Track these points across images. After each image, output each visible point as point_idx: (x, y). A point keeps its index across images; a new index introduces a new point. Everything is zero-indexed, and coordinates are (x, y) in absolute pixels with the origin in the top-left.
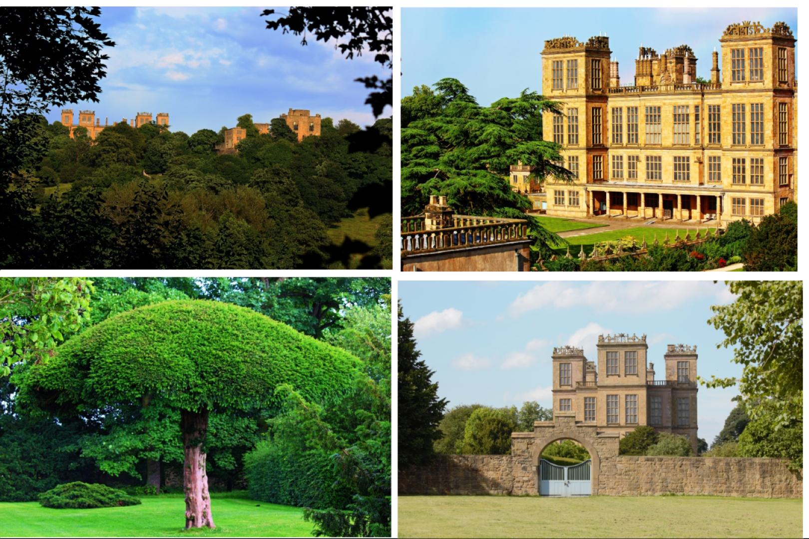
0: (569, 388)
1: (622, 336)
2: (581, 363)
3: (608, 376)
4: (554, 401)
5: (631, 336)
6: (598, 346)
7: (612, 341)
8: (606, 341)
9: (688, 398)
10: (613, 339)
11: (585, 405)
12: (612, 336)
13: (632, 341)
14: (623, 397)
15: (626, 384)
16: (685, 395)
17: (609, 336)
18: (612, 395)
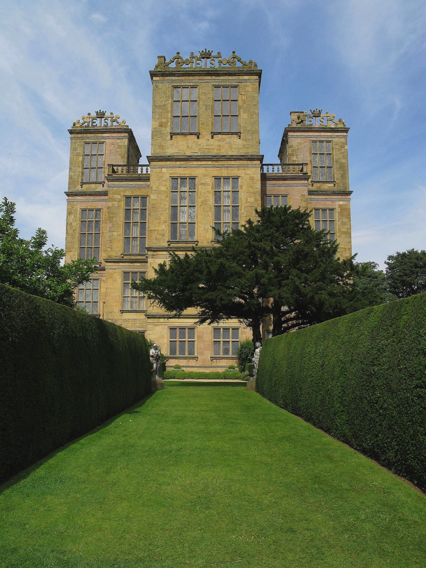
0: (100, 188)
1: (206, 55)
2: (126, 141)
3: (172, 135)
4: (69, 213)
5: (227, 56)
6: (153, 75)
7: (184, 66)
8: (173, 65)
9: (332, 210)
10: (187, 62)
11: (127, 211)
12: (186, 57)
13: (227, 65)
14: (210, 181)
15: (214, 152)
16: (329, 204)
17: (178, 57)
18: (183, 179)
